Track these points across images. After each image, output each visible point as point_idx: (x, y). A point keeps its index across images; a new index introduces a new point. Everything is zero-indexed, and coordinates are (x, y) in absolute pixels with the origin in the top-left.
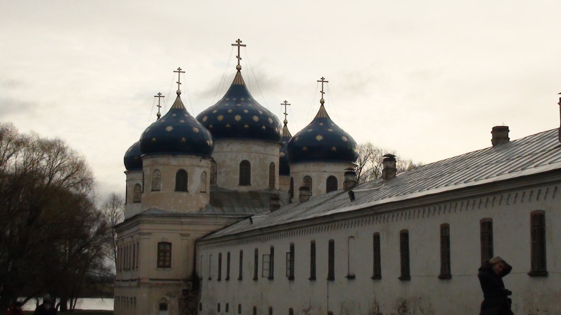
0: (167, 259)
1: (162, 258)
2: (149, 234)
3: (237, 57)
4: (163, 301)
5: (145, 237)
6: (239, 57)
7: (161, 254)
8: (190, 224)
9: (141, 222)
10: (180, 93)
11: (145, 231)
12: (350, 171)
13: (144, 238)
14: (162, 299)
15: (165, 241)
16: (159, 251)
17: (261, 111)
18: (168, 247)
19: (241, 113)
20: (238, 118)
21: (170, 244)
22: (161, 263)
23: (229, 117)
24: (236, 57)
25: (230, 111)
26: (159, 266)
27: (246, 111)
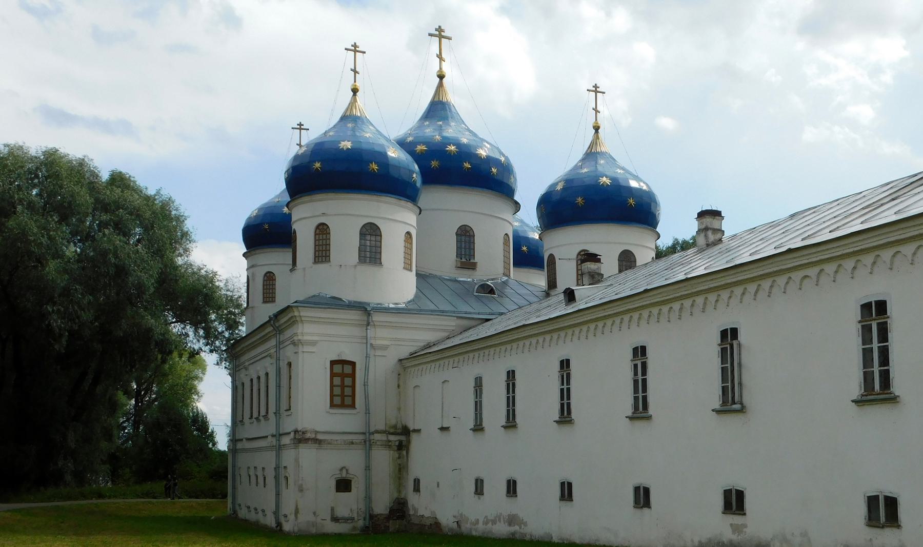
0: (348, 391)
1: (337, 391)
2: (314, 343)
4: (344, 474)
7: (337, 381)
9: (298, 319)
10: (358, 91)
11: (306, 338)
14: (341, 469)
15: (344, 358)
16: (333, 375)
18: (348, 369)
21: (353, 364)
22: (337, 400)
24: (436, 55)
26: (332, 405)
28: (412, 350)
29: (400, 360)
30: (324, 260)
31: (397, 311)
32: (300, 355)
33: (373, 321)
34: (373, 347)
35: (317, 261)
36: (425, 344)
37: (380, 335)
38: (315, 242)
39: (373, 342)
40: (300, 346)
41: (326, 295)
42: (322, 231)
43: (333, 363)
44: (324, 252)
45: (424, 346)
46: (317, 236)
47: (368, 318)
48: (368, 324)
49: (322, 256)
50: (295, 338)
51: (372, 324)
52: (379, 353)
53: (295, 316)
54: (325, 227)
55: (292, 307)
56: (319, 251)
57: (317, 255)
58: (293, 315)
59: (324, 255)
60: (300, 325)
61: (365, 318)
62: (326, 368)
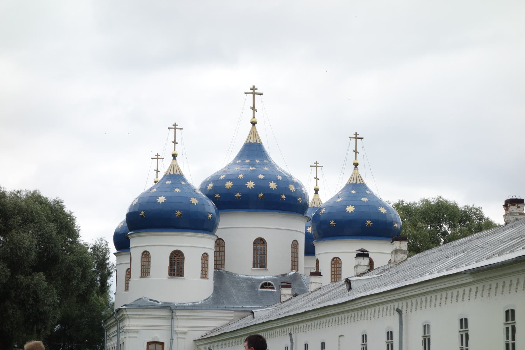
2: (136, 331)
3: (252, 108)
5: (131, 335)
6: (253, 109)
8: (187, 318)
9: (126, 316)
11: (131, 328)
12: (362, 252)
13: (129, 337)
15: (156, 340)
17: (280, 176)
19: (255, 179)
20: (250, 185)
21: (162, 344)
23: (239, 184)
25: (241, 176)
27: (261, 176)
28: (203, 333)
29: (195, 341)
30: (146, 275)
31: (194, 308)
32: (127, 338)
33: (176, 316)
34: (176, 332)
35: (142, 275)
36: (211, 329)
37: (181, 325)
38: (142, 263)
39: (176, 329)
40: (127, 333)
41: (147, 298)
42: (146, 255)
43: (149, 343)
44: (147, 270)
45: (212, 331)
46: (143, 259)
47: (172, 314)
48: (172, 318)
49: (145, 273)
50: (125, 329)
51: (175, 317)
52: (180, 336)
53: (124, 314)
54: (148, 253)
55: (122, 309)
56: (144, 269)
57: (142, 272)
58: (123, 314)
59: (147, 271)
60: (127, 320)
61: (170, 314)
62: (144, 347)
